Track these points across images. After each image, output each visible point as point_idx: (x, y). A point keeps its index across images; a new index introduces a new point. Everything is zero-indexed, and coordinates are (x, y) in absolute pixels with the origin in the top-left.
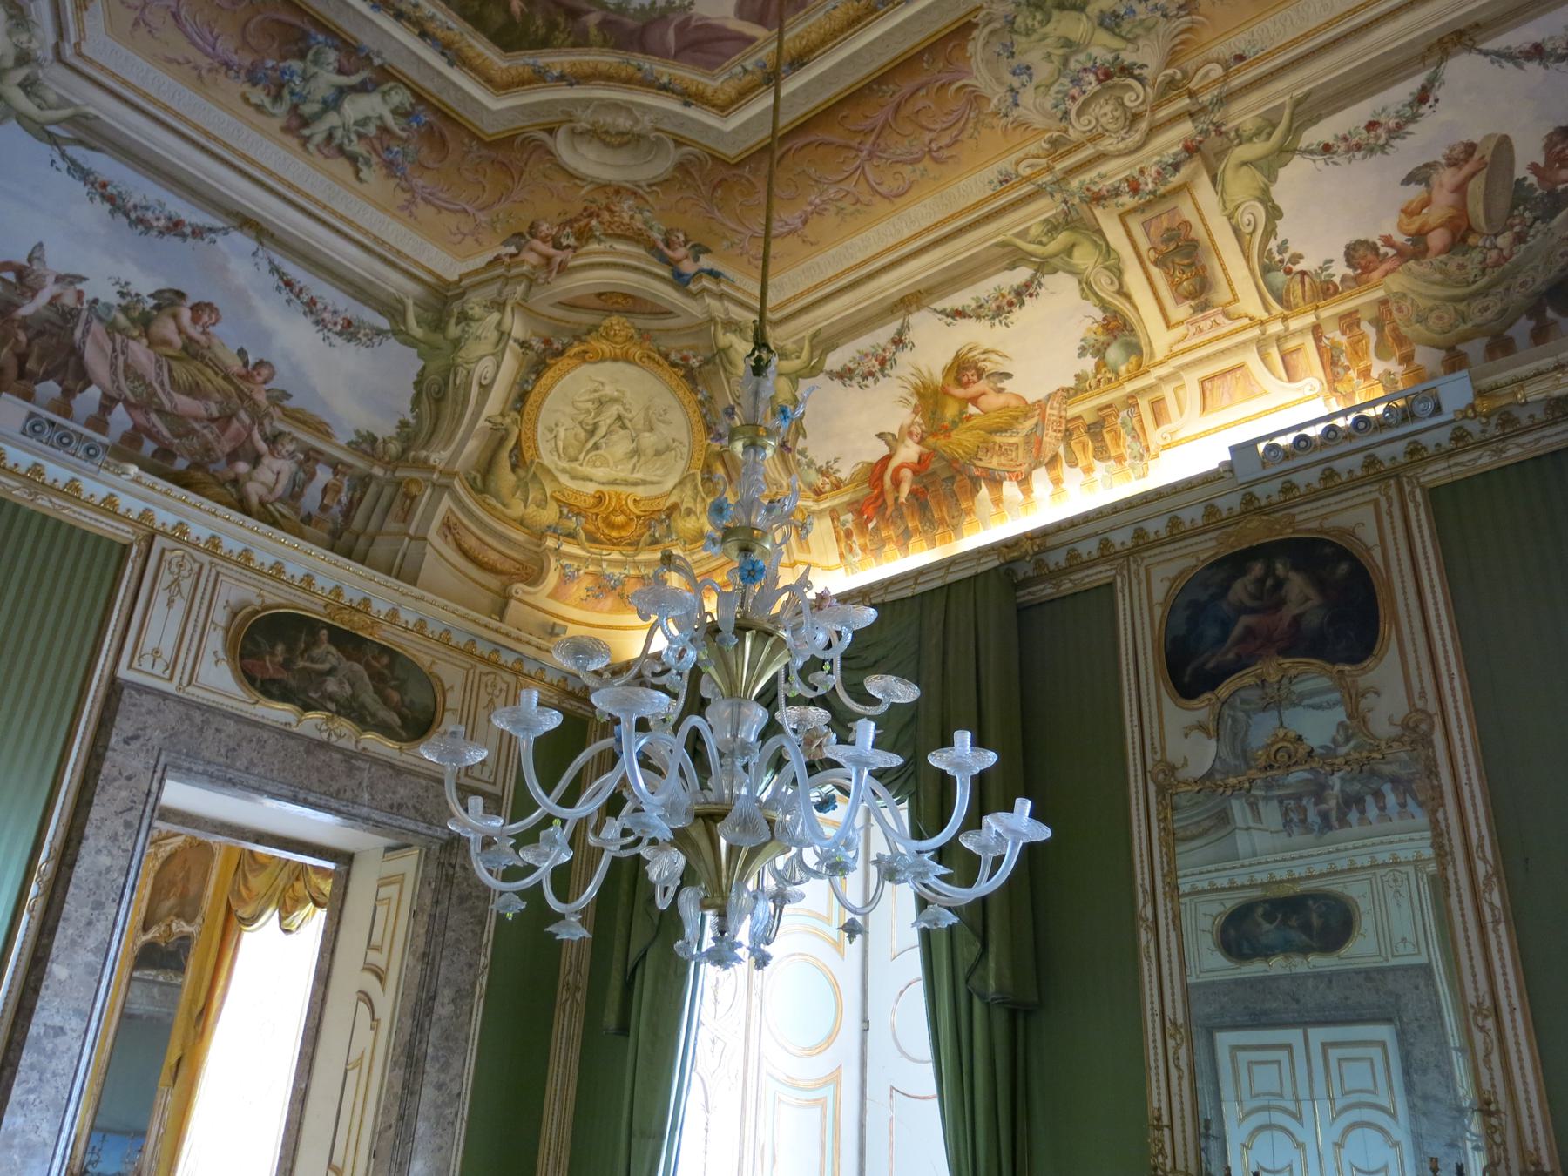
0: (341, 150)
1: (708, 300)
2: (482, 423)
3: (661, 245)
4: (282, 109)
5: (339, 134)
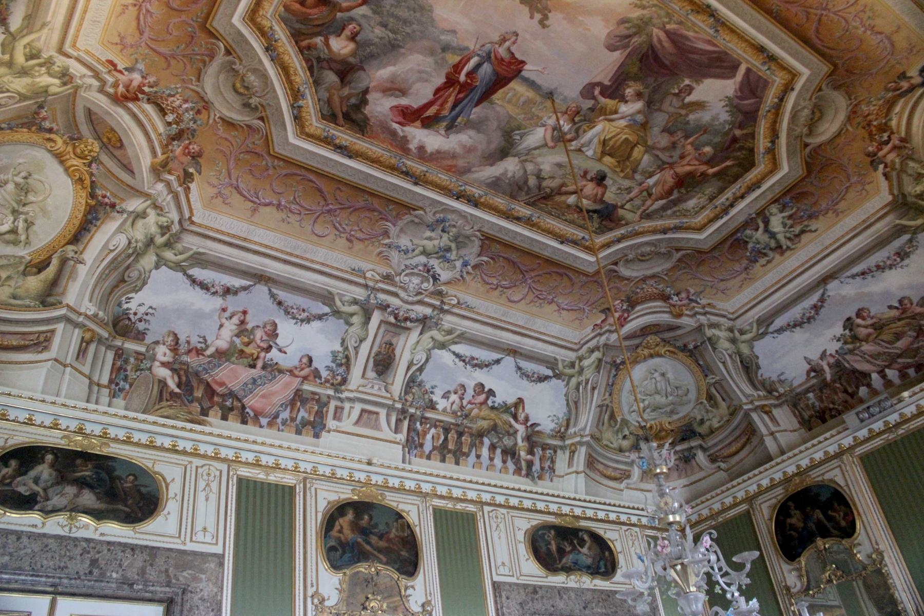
0: (797, 236)
4: (771, 254)
5: (788, 235)
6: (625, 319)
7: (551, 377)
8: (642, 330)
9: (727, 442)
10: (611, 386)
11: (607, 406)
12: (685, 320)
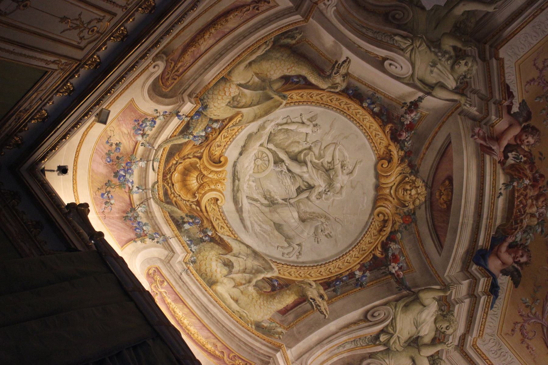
1: (466, 283)
2: (347, 53)
3: (510, 240)
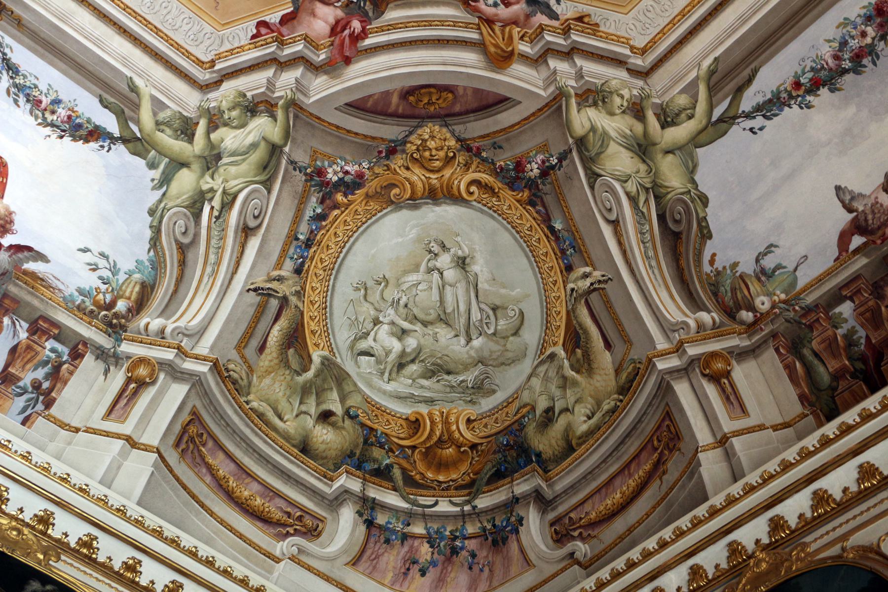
6: (356, 38)
7: (113, 139)
8: (407, 93)
9: (604, 477)
10: (303, 247)
11: (284, 301)
12: (521, 78)
